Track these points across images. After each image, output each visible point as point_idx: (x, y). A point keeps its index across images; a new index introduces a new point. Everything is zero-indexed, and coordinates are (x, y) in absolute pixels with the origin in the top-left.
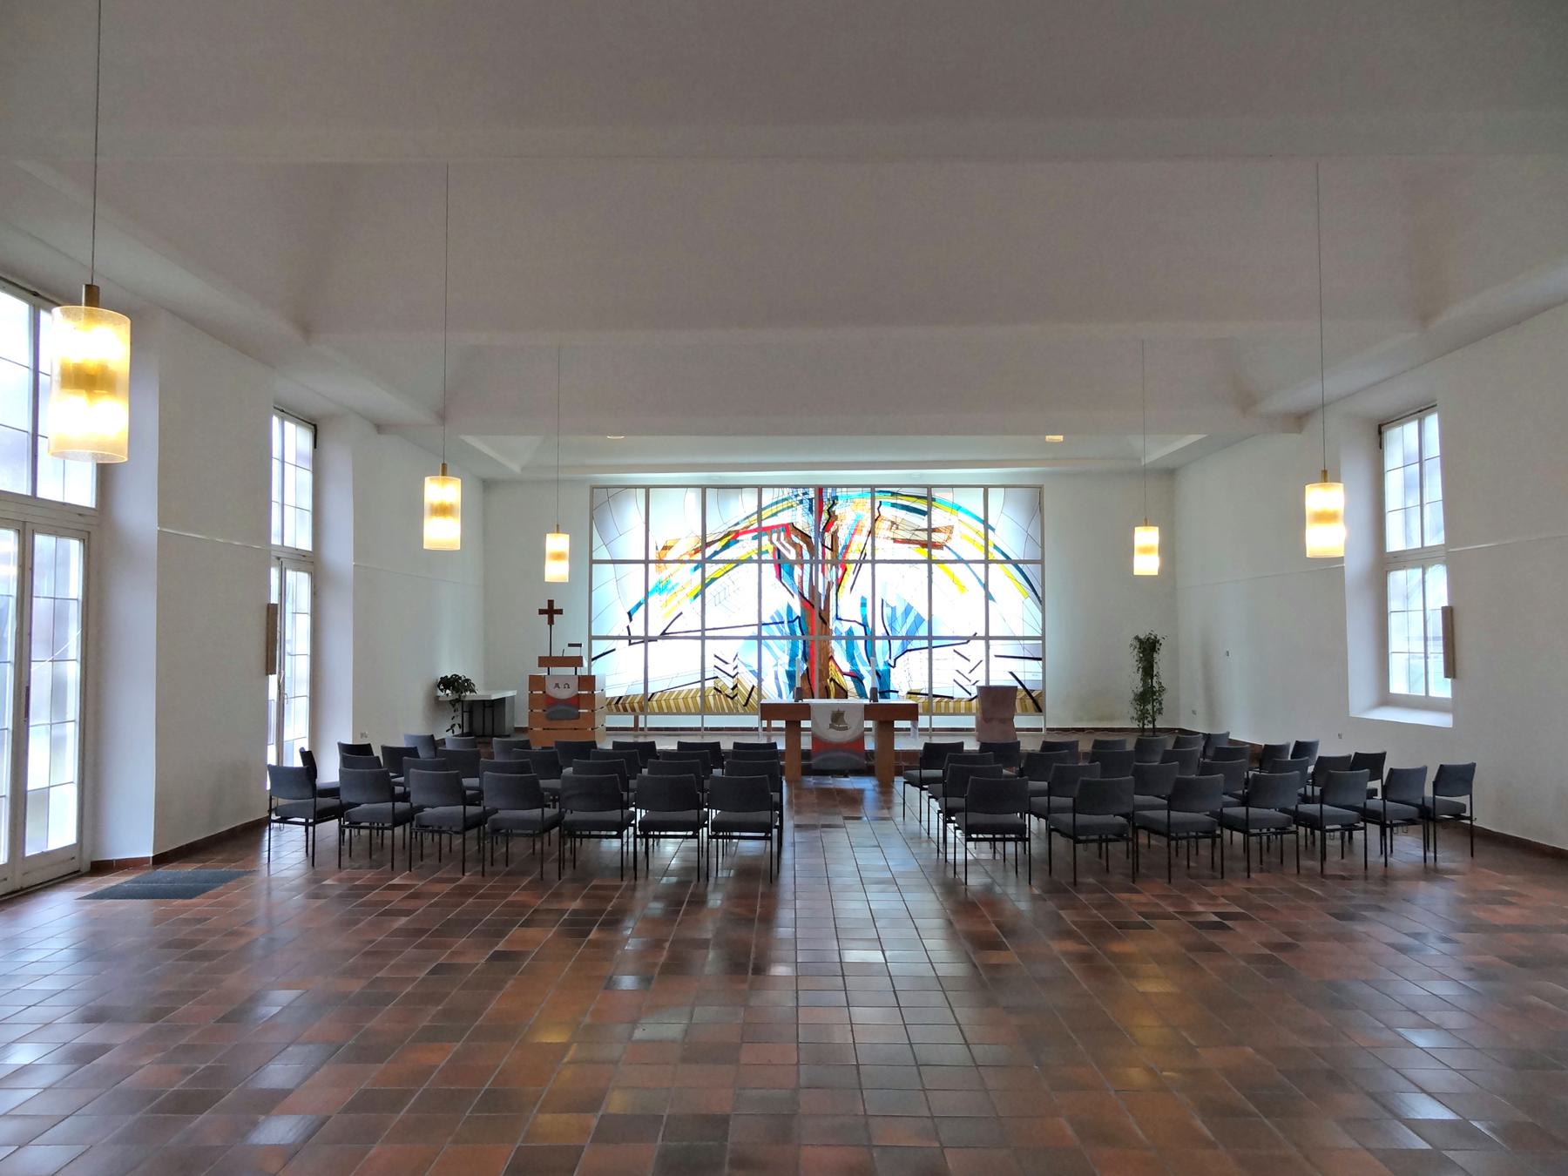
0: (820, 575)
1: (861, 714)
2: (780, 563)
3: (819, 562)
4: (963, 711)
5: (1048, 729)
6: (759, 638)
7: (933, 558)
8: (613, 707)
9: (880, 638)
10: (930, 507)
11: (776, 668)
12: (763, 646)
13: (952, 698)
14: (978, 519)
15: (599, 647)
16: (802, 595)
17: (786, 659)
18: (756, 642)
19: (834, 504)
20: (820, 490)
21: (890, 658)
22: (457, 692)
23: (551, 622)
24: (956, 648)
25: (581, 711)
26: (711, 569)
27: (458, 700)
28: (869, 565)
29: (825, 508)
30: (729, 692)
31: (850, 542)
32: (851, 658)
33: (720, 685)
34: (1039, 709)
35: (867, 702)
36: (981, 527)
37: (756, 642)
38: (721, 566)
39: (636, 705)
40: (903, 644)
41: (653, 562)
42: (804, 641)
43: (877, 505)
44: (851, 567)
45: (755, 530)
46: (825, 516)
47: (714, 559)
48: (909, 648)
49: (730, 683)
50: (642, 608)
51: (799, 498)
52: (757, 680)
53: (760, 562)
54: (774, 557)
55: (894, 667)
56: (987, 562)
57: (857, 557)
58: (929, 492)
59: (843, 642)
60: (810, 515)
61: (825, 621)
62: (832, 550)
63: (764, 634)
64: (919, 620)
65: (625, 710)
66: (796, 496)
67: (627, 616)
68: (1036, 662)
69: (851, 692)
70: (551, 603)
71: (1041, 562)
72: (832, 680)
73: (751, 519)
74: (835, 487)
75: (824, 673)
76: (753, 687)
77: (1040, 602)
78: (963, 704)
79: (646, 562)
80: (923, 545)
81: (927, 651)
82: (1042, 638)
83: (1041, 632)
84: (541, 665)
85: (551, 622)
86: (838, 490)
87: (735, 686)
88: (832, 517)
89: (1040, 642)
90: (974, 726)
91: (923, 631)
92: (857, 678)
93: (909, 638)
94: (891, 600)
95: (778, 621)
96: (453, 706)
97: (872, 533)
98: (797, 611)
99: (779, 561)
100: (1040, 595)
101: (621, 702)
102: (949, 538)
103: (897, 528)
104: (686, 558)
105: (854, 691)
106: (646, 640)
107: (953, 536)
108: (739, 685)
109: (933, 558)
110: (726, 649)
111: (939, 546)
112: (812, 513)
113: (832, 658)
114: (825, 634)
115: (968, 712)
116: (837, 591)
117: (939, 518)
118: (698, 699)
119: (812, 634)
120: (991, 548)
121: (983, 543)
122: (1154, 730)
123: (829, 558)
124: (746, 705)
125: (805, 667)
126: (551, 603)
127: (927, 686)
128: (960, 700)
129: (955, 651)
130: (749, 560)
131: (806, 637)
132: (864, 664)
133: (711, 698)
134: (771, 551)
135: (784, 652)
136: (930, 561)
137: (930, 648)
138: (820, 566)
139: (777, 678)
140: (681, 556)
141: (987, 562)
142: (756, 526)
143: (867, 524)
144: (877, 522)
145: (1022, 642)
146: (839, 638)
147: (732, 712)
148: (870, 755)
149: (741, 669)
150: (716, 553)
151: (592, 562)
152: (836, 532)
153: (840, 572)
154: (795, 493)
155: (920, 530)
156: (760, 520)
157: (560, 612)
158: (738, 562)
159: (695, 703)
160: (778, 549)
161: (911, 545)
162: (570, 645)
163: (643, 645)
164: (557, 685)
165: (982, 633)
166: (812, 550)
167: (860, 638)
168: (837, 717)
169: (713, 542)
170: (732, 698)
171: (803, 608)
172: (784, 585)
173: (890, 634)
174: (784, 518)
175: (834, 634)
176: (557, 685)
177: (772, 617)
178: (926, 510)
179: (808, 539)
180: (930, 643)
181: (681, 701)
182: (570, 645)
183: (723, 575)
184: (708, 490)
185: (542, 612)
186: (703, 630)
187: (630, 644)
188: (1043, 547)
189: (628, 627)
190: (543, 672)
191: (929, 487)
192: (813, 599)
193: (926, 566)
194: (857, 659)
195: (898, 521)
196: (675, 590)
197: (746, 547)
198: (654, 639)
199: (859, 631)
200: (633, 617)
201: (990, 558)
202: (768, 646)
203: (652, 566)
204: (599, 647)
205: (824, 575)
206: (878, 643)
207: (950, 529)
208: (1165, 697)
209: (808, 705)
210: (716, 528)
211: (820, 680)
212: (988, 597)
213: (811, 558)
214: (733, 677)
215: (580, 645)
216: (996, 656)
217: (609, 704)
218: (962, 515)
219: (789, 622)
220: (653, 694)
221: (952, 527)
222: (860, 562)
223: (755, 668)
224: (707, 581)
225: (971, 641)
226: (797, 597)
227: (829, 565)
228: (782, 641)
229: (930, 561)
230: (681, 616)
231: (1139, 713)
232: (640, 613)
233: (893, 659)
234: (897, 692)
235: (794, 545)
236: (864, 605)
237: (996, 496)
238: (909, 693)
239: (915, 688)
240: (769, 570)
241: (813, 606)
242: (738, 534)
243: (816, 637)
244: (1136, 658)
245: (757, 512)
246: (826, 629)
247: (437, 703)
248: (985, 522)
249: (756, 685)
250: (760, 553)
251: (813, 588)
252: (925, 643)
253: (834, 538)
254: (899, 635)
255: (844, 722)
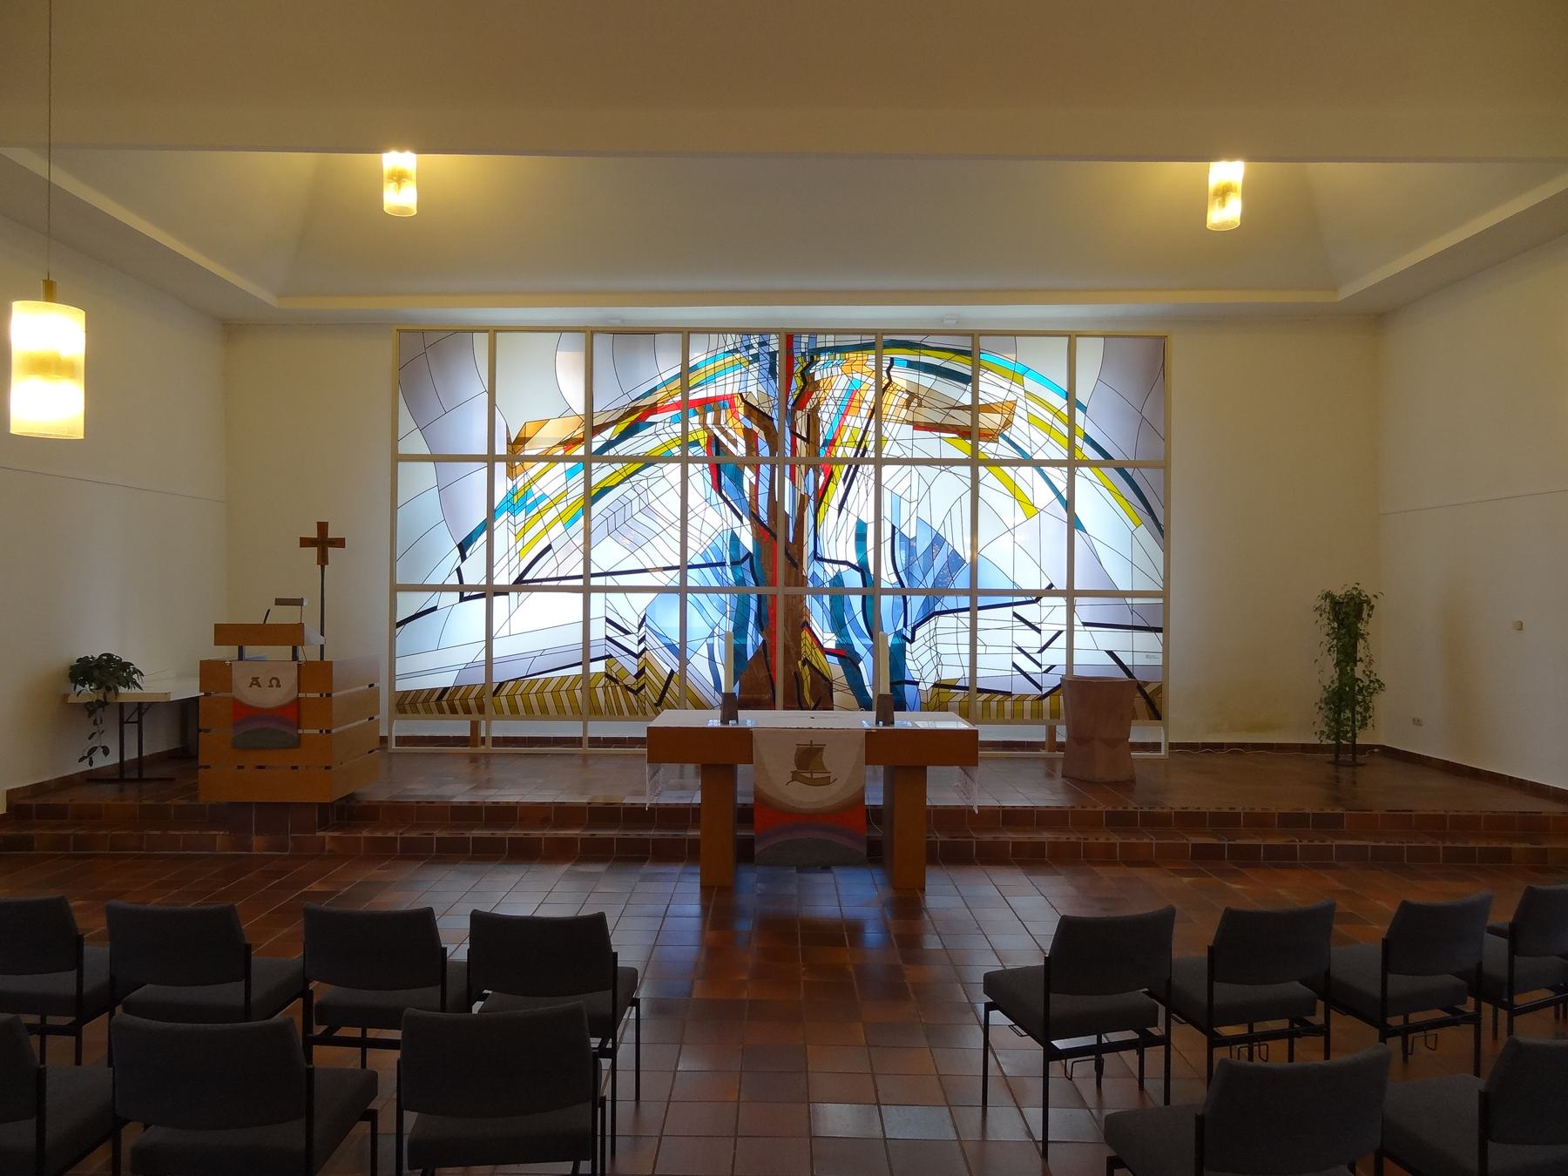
0: (787, 481)
1: (858, 750)
2: (721, 468)
3: (785, 461)
4: (1027, 717)
5: (1172, 746)
6: (683, 590)
7: (981, 456)
8: (433, 705)
9: (887, 592)
10: (977, 366)
11: (710, 641)
12: (690, 608)
13: (1009, 694)
14: (1054, 387)
15: (409, 604)
16: (755, 517)
17: (727, 625)
18: (676, 598)
19: (812, 363)
20: (789, 339)
21: (905, 625)
22: (103, 690)
23: (323, 560)
24: (1018, 609)
25: (306, 731)
26: (601, 473)
27: (103, 704)
28: (871, 467)
29: (798, 369)
30: (630, 681)
31: (840, 427)
32: (838, 625)
33: (615, 669)
34: (1156, 714)
35: (867, 720)
36: (1060, 403)
37: (676, 598)
38: (618, 466)
39: (472, 703)
40: (926, 604)
41: (501, 458)
42: (759, 597)
43: (886, 365)
44: (840, 471)
45: (678, 405)
46: (797, 383)
47: (606, 454)
48: (937, 608)
49: (632, 666)
50: (484, 537)
51: (752, 352)
52: (678, 662)
53: (685, 461)
54: (709, 452)
55: (912, 641)
56: (1072, 464)
57: (850, 452)
58: (975, 343)
59: (826, 599)
60: (772, 381)
61: (795, 561)
62: (807, 440)
63: (691, 583)
64: (955, 561)
65: (453, 711)
66: (749, 347)
67: (457, 552)
68: (1153, 634)
69: (840, 684)
70: (322, 527)
71: (1164, 465)
72: (806, 662)
73: (671, 387)
74: (813, 333)
75: (793, 651)
76: (672, 672)
77: (1161, 531)
78: (1027, 705)
79: (490, 459)
80: (964, 433)
81: (967, 614)
82: (1164, 594)
83: (1161, 584)
84: (218, 642)
85: (323, 560)
86: (820, 338)
87: (641, 672)
88: (810, 385)
89: (1161, 601)
90: (1043, 739)
91: (962, 581)
92: (847, 656)
93: (935, 593)
94: (909, 530)
95: (715, 561)
96: (91, 713)
97: (876, 412)
98: (747, 541)
99: (717, 460)
100: (1161, 521)
101: (447, 695)
102: (1008, 423)
103: (920, 405)
104: (560, 452)
105: (844, 680)
106: (489, 592)
107: (1016, 420)
108: (647, 670)
109: (981, 456)
110: (629, 608)
111: (992, 436)
112: (775, 379)
113: (807, 625)
114: (796, 585)
115: (1037, 715)
116: (817, 510)
117: (992, 388)
118: (578, 692)
119: (774, 583)
120: (1079, 441)
121: (1065, 430)
122: (1356, 749)
123: (804, 455)
124: (656, 705)
125: (761, 639)
126: (322, 527)
127: (967, 675)
128: (1023, 698)
129: (1015, 615)
130: (669, 459)
131: (765, 590)
132: (860, 635)
133: (600, 692)
134: (702, 442)
135: (725, 615)
136: (974, 462)
137: (973, 609)
138: (788, 468)
139: (711, 658)
140: (550, 449)
141: (1072, 464)
142: (678, 398)
143: (870, 396)
144: (887, 394)
145: (1129, 601)
146: (818, 592)
147: (636, 713)
148: (875, 814)
149: (652, 641)
150: (610, 444)
151: (397, 458)
152: (816, 409)
153: (822, 479)
154: (746, 343)
155: (958, 408)
156: (686, 388)
157: (340, 543)
158: (648, 461)
159: (573, 700)
160: (717, 438)
161: (943, 435)
162: (279, 602)
163: (484, 600)
164: (255, 681)
165: (1061, 585)
166: (773, 441)
167: (854, 591)
168: (809, 755)
169: (605, 426)
170: (636, 693)
171: (757, 540)
172: (725, 500)
173: (906, 587)
174: (728, 385)
175: (811, 585)
176: (255, 681)
177: (704, 555)
178: (969, 373)
179: (767, 422)
180: (973, 601)
181: (548, 697)
182: (279, 602)
183: (621, 482)
184: (597, 338)
185: (305, 542)
186: (587, 575)
187: (462, 599)
188: (1166, 438)
189: (458, 570)
190: (227, 653)
191: (974, 335)
192: (776, 524)
193: (966, 471)
194: (848, 626)
195: (922, 392)
196: (541, 506)
197: (661, 433)
198: (503, 591)
199: (853, 579)
200: (468, 554)
201: (1078, 456)
202: (701, 608)
203: (501, 468)
204: (409, 604)
205: (794, 484)
206: (886, 602)
207: (1009, 409)
208: (1381, 702)
209: (747, 734)
210: (609, 401)
211: (785, 664)
212: (1074, 524)
213: (772, 453)
214: (637, 656)
215: (299, 602)
216: (1085, 624)
217: (426, 700)
218: (1030, 385)
219: (734, 563)
220: (501, 684)
221: (1014, 404)
222: (854, 464)
223: (676, 639)
224: (594, 492)
225: (1045, 600)
226: (746, 521)
227: (803, 467)
228: (722, 596)
229: (974, 462)
230: (550, 553)
231: (1333, 724)
232: (478, 549)
233: (909, 628)
234: (917, 683)
235: (749, 435)
236: (861, 537)
237: (1091, 354)
238: (935, 685)
239: (949, 674)
240: (700, 478)
241: (775, 536)
242: (653, 409)
243: (781, 590)
244: (1327, 629)
245: (680, 375)
246: (797, 575)
247: (68, 709)
248: (1070, 396)
249: (676, 669)
250: (686, 443)
251: (774, 506)
252: (965, 602)
253: (813, 421)
254: (921, 586)
255: (822, 768)
